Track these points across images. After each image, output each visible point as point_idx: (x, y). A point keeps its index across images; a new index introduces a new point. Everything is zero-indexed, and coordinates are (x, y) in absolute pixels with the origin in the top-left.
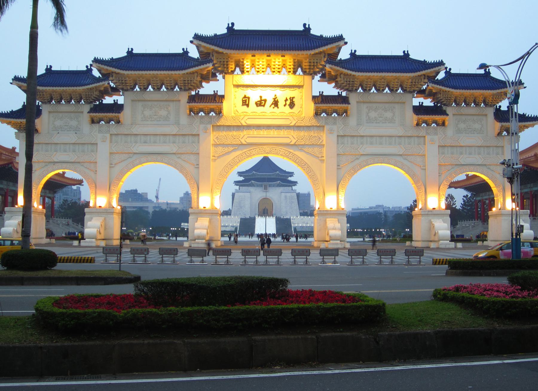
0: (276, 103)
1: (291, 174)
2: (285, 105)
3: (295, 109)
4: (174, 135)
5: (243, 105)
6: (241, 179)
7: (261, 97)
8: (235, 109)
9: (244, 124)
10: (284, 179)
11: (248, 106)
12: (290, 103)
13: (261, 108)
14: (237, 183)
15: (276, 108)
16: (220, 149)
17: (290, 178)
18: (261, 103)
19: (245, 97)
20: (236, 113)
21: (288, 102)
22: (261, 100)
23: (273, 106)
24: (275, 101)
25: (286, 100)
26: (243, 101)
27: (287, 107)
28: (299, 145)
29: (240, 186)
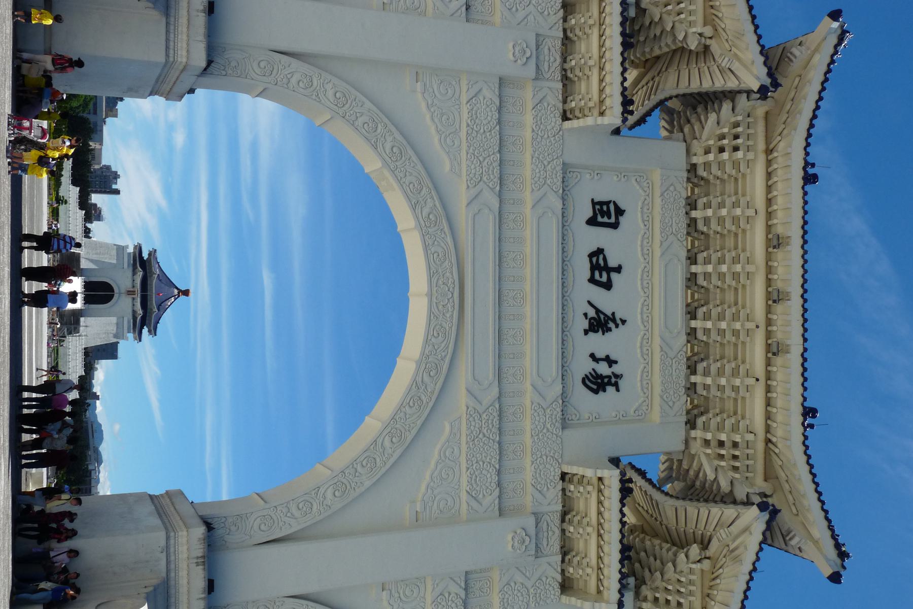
0: (600, 323)
1: (153, 331)
2: (592, 356)
3: (583, 397)
5: (594, 203)
6: (145, 255)
7: (618, 269)
10: (145, 320)
11: (592, 222)
12: (601, 377)
14: (139, 248)
15: (585, 324)
17: (145, 330)
18: (602, 270)
19: (620, 212)
21: (603, 369)
22: (609, 270)
23: (592, 313)
25: (610, 362)
26: (608, 203)
27: (588, 366)
29: (134, 253)
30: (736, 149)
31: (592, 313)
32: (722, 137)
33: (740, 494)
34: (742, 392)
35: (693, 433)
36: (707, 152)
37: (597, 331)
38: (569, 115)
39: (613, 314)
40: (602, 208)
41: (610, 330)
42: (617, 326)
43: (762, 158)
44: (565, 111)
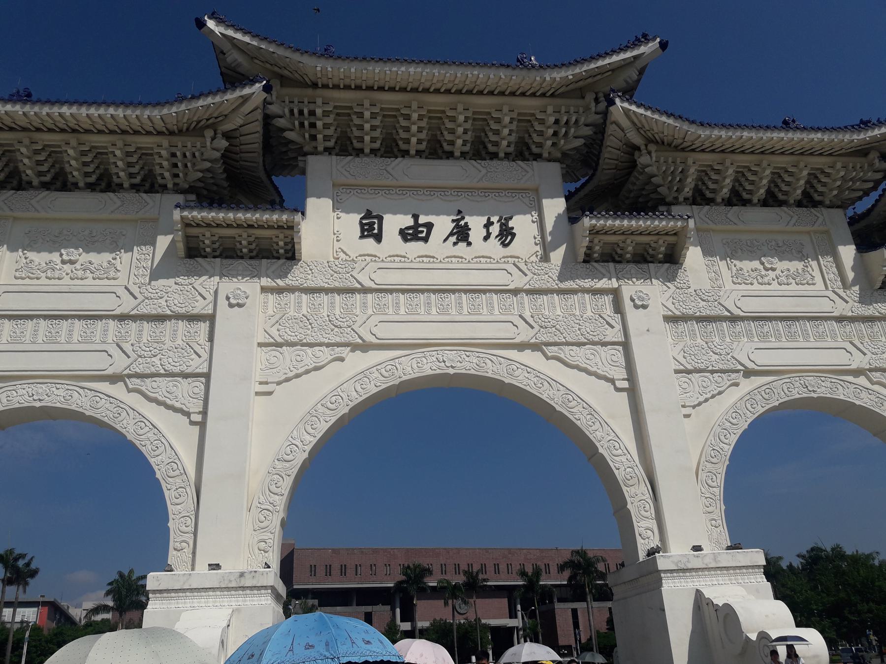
0: (461, 234)
2: (486, 238)
4: (122, 318)
5: (362, 237)
8: (337, 245)
9: (368, 284)
11: (378, 238)
13: (416, 247)
15: (462, 245)
16: (287, 359)
20: (342, 255)
21: (495, 229)
22: (417, 225)
23: (453, 239)
24: (457, 226)
26: (362, 225)
28: (548, 344)
30: (312, 113)
31: (453, 239)
32: (302, 125)
33: (598, 118)
34: (469, 114)
35: (546, 155)
36: (313, 138)
37: (468, 235)
38: (290, 255)
39: (453, 221)
40: (366, 230)
41: (466, 223)
42: (463, 218)
43: (319, 92)
44: (287, 258)
